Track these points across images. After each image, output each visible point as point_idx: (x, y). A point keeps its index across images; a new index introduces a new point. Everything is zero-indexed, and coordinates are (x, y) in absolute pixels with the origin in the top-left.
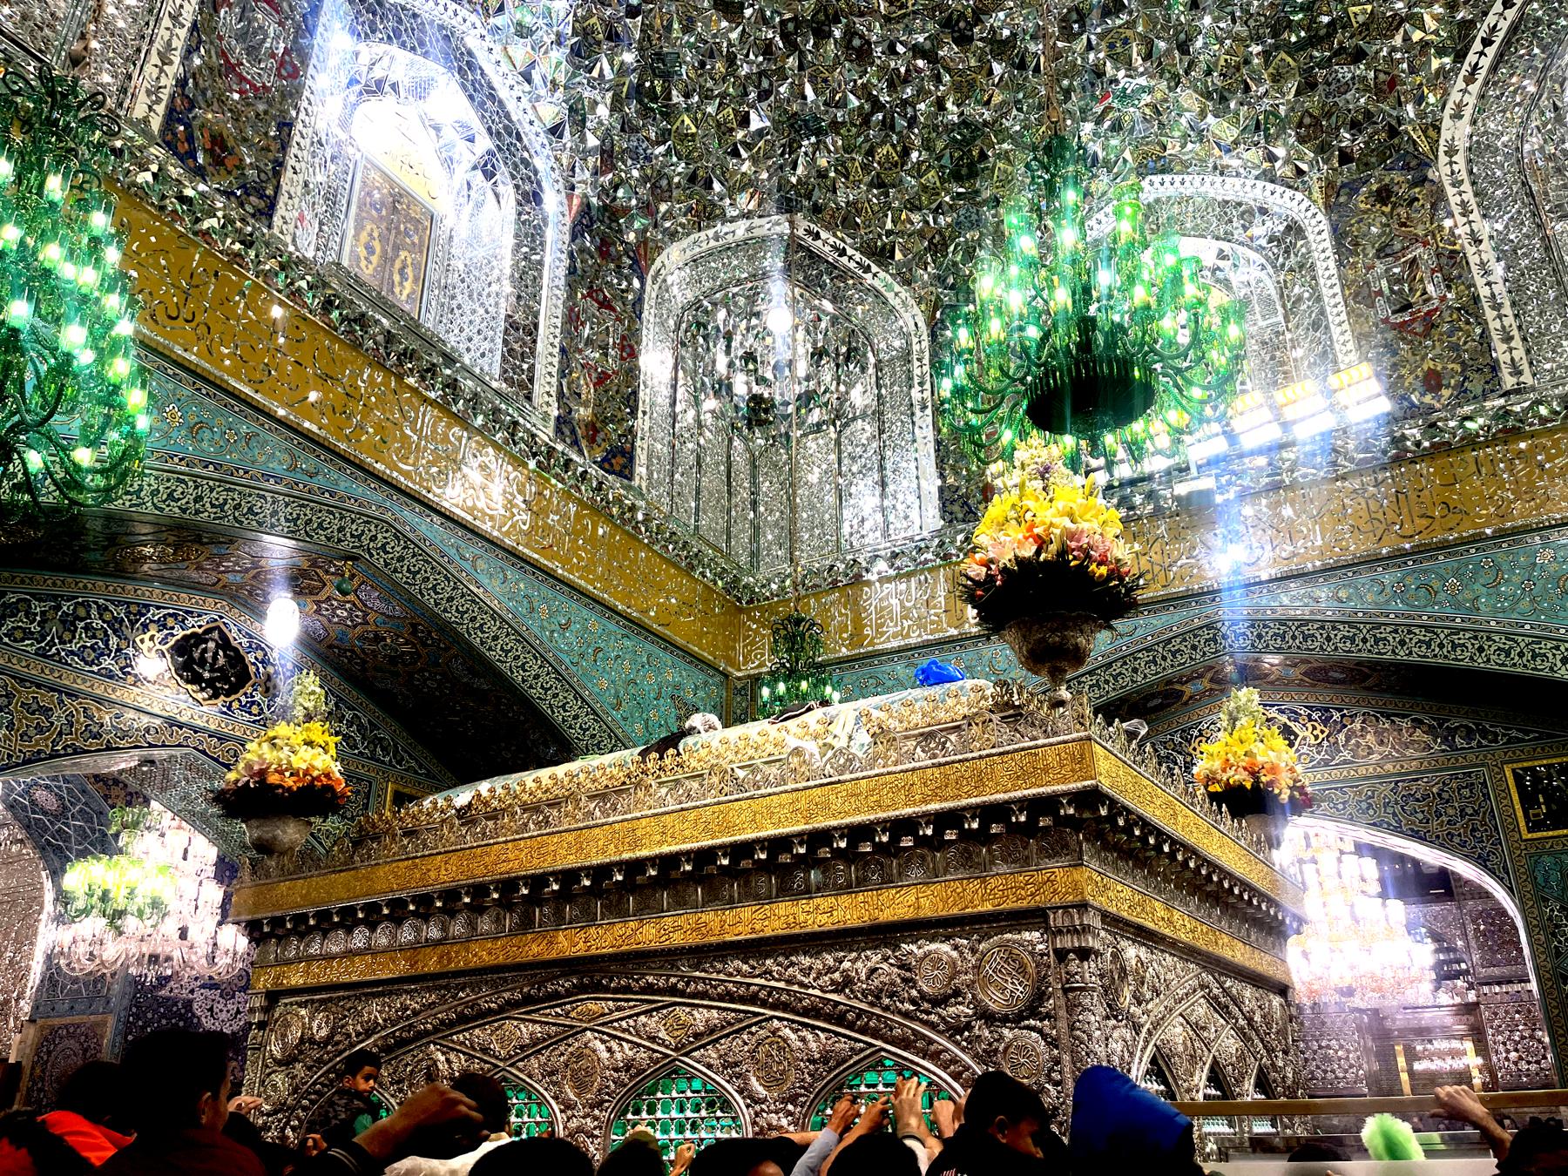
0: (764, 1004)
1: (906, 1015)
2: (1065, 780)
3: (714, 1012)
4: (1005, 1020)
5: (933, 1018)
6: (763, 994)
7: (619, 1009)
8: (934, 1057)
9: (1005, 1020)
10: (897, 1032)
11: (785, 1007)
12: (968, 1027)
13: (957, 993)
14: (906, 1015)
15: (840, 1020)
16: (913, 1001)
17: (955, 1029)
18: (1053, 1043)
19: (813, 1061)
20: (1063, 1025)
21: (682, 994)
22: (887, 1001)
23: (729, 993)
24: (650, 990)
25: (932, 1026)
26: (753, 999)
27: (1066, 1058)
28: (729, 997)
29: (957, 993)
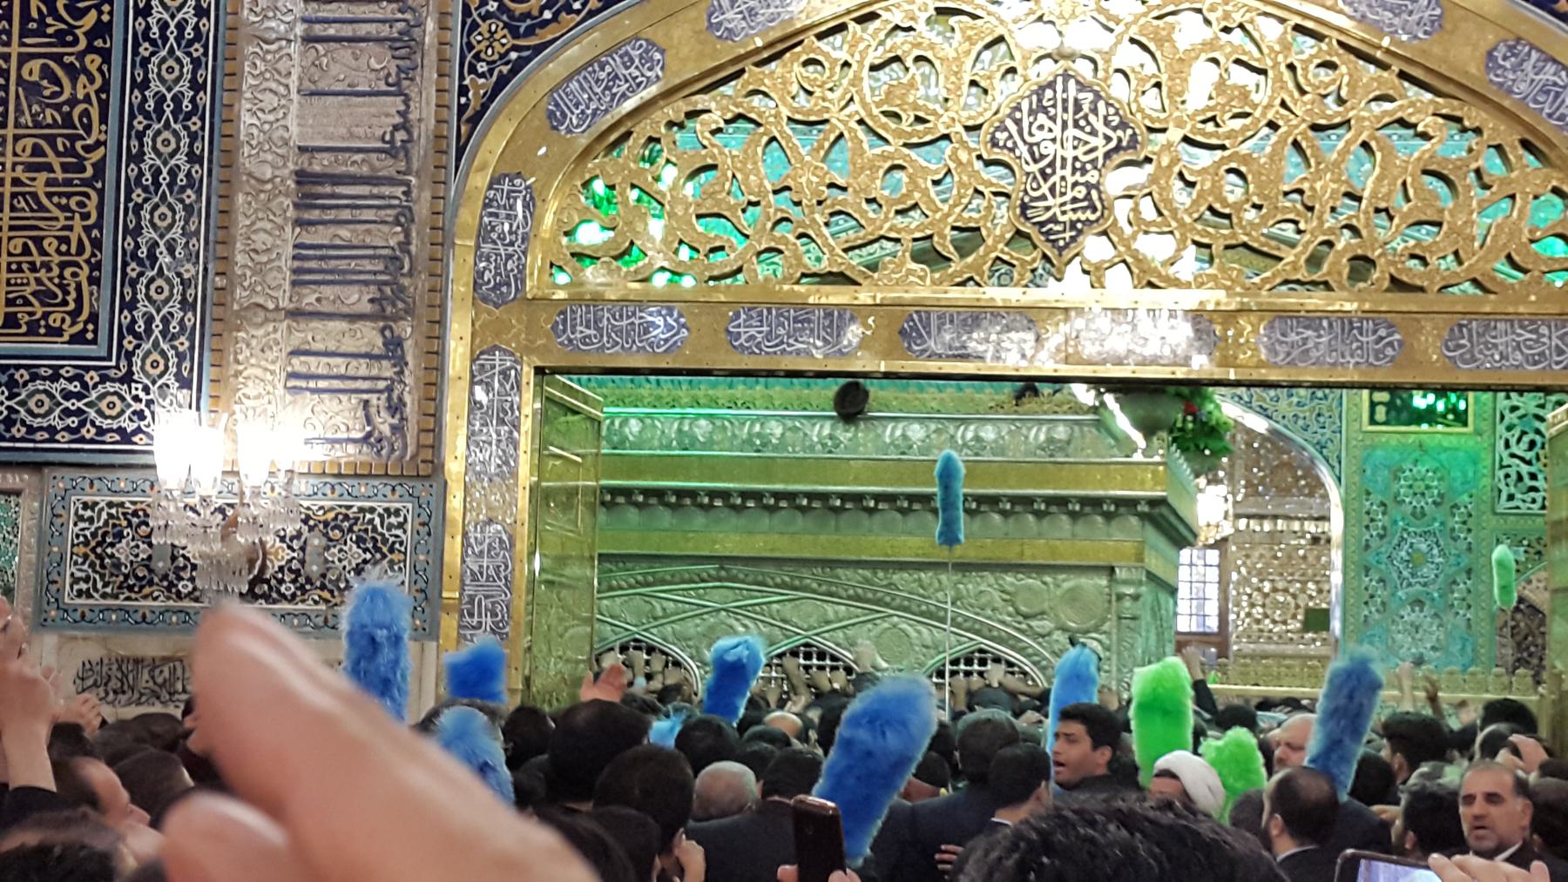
0: (887, 605)
1: (1003, 623)
2: (1142, 486)
3: (843, 608)
5: (1024, 626)
6: (888, 599)
8: (1021, 651)
10: (995, 633)
11: (906, 609)
12: (1049, 634)
13: (1043, 613)
14: (1003, 623)
16: (1010, 615)
18: (1107, 649)
19: (927, 647)
20: (1114, 637)
21: (814, 592)
22: (989, 612)
24: (784, 585)
26: (878, 602)
27: (1114, 658)
28: (858, 598)
29: (1043, 613)
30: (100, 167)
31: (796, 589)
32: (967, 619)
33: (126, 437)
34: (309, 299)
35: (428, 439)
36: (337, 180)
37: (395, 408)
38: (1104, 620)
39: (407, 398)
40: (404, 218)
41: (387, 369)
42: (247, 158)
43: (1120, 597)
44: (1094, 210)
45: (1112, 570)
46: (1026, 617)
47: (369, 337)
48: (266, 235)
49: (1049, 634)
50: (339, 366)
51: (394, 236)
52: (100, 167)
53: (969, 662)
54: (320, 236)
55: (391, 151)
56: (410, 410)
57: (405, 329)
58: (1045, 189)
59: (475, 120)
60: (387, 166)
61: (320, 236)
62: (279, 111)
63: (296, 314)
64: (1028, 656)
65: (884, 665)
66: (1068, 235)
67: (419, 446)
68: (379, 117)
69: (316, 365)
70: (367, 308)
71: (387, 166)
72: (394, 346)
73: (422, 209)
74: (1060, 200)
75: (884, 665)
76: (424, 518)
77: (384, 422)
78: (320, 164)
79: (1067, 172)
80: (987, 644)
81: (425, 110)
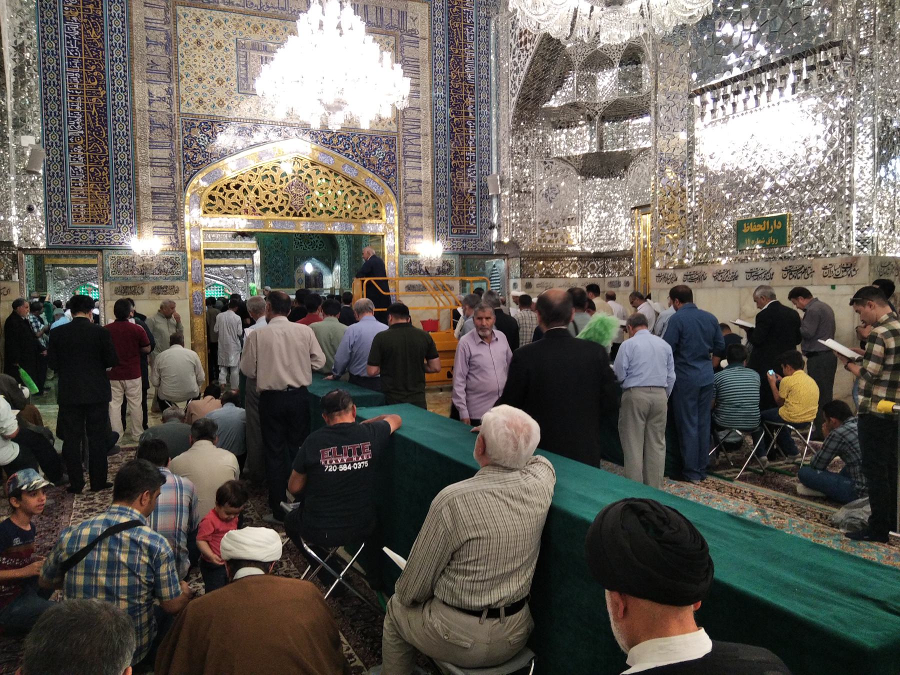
30: (109, 190)
33: (120, 244)
34: (156, 217)
36: (160, 194)
37: (176, 238)
40: (175, 201)
41: (174, 230)
42: (141, 189)
47: (169, 224)
48: (147, 205)
50: (164, 230)
51: (173, 205)
52: (109, 190)
54: (157, 204)
55: (171, 188)
57: (177, 223)
59: (187, 183)
60: (170, 191)
61: (157, 204)
62: (147, 180)
63: (154, 220)
68: (167, 182)
69: (158, 229)
70: (168, 218)
71: (170, 191)
72: (175, 226)
77: (174, 241)
78: (155, 191)
81: (178, 180)
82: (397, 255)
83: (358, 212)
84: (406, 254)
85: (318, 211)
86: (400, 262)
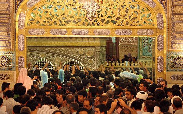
0: (57, 54)
1: (77, 56)
4: (89, 58)
5: (80, 57)
7: (33, 53)
8: (80, 61)
9: (89, 58)
12: (85, 58)
15: (68, 56)
16: (78, 55)
17: (82, 58)
21: (44, 52)
23: (39, 50)
25: (80, 58)
26: (55, 53)
28: (51, 53)
31: (40, 51)
32: (70, 56)
35: (14, 46)
38: (94, 56)
39: (11, 41)
43: (96, 52)
44: (95, 16)
45: (95, 47)
46: (80, 55)
49: (85, 58)
53: (71, 63)
56: (11, 43)
58: (89, 13)
64: (81, 62)
65: (56, 64)
66: (92, 19)
67: (13, 47)
73: (11, 18)
74: (91, 15)
75: (56, 64)
76: (13, 56)
79: (92, 12)
80: (74, 60)
82: (165, 52)
83: (136, 20)
84: (172, 52)
85: (106, 21)
86: (167, 58)
